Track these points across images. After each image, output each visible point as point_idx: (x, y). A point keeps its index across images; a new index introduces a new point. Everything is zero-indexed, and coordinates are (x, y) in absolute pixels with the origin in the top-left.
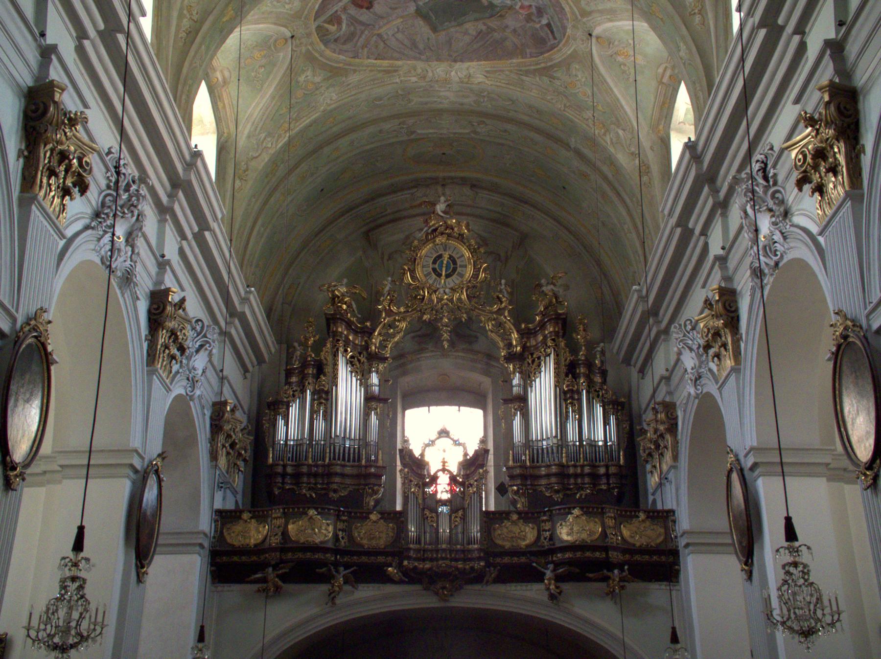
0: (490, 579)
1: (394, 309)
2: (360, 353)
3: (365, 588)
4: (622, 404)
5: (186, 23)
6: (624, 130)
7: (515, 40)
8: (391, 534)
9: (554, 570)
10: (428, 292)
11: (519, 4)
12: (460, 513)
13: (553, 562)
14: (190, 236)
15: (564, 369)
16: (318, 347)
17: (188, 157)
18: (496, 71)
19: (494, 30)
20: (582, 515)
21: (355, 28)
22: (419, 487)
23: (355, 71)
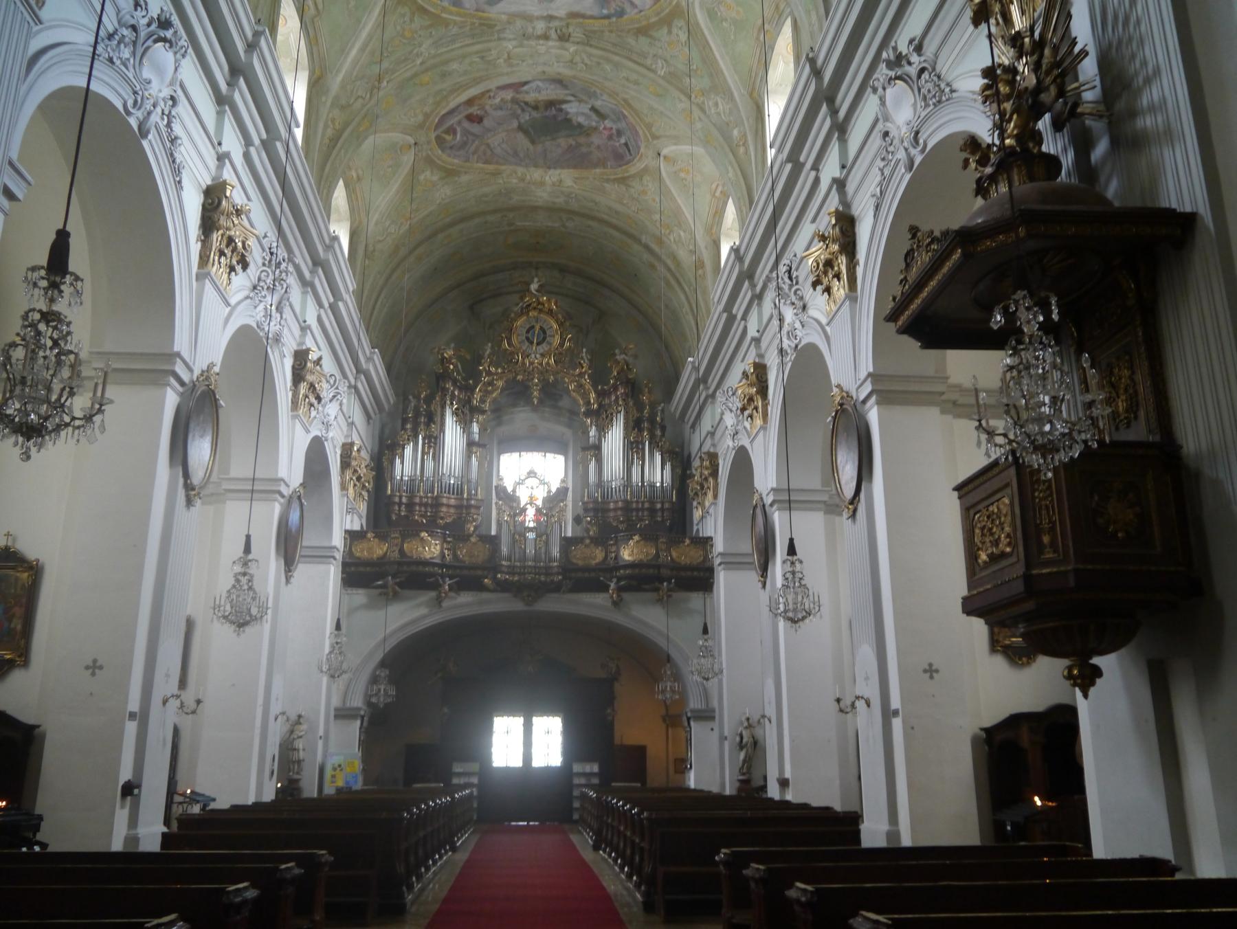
1: (492, 370)
4: (676, 454)
5: (329, 132)
6: (684, 232)
9: (617, 583)
11: (603, 126)
12: (544, 537)
13: (616, 577)
14: (326, 305)
15: (632, 424)
16: (429, 400)
17: (327, 241)
21: (467, 138)
23: (466, 173)
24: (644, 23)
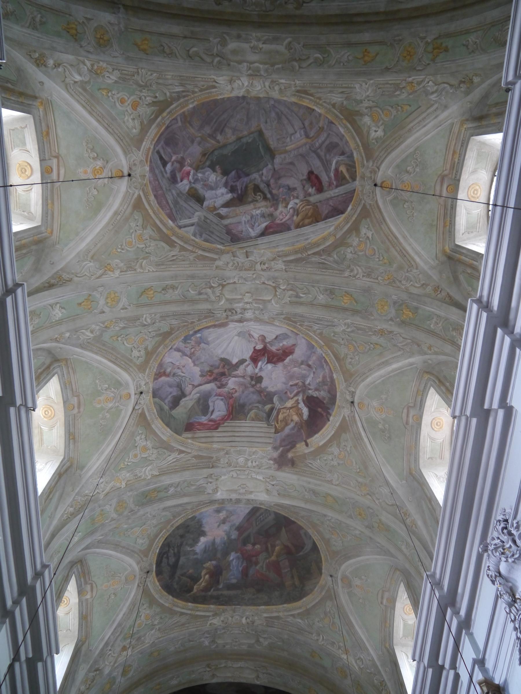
6: (76, 82)
7: (192, 130)
11: (191, 177)
18: (207, 89)
19: (210, 136)
21: (325, 156)
23: (334, 105)
24: (167, 341)
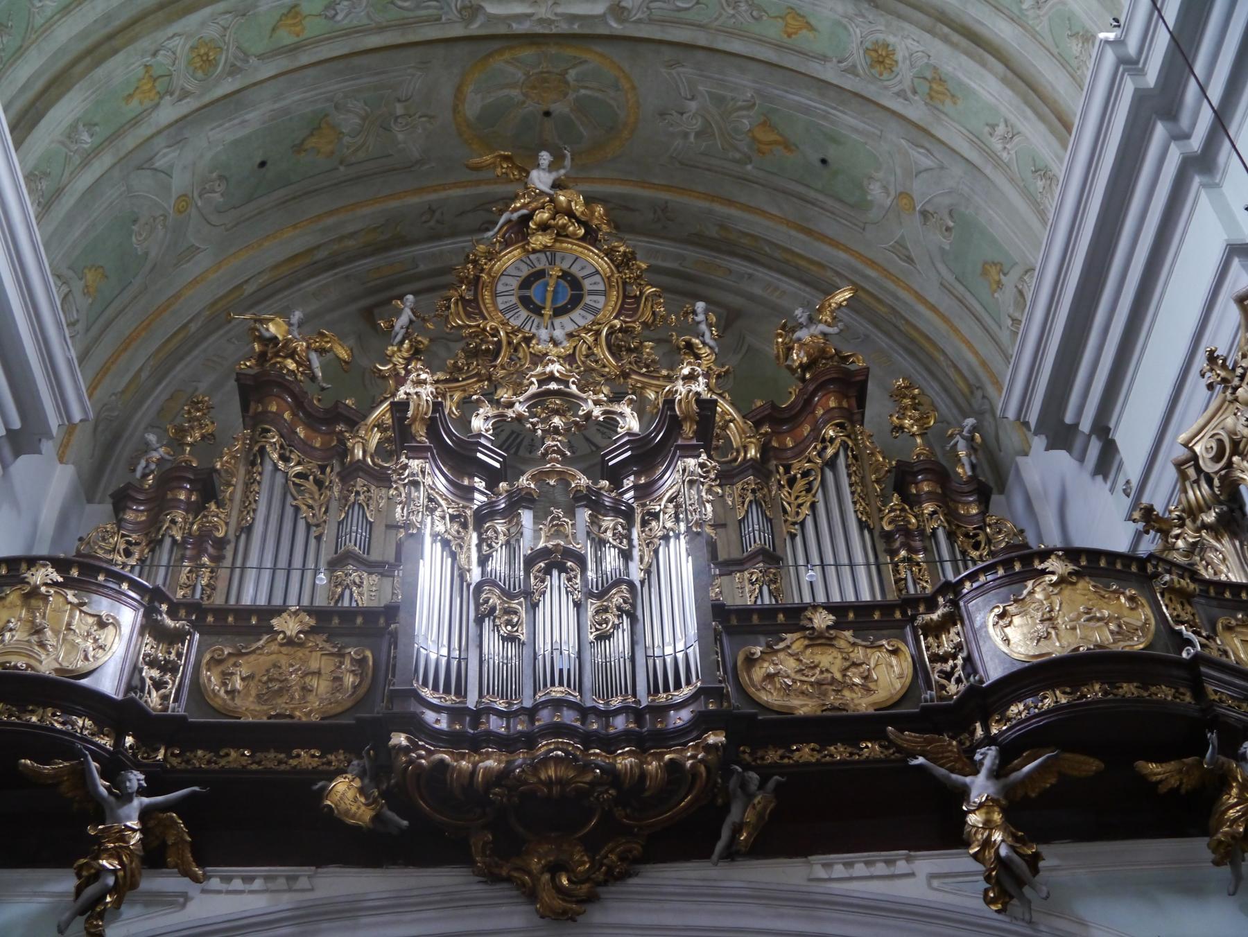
0: (750, 817)
2: (323, 469)
3: (237, 884)
8: (349, 680)
9: (997, 774)
10: (509, 343)
13: (989, 740)
20: (1078, 574)
22: (464, 526)
